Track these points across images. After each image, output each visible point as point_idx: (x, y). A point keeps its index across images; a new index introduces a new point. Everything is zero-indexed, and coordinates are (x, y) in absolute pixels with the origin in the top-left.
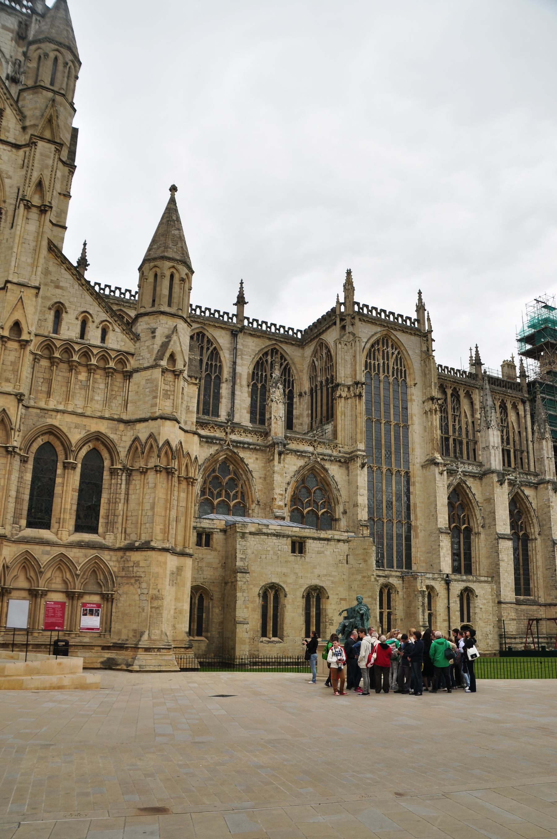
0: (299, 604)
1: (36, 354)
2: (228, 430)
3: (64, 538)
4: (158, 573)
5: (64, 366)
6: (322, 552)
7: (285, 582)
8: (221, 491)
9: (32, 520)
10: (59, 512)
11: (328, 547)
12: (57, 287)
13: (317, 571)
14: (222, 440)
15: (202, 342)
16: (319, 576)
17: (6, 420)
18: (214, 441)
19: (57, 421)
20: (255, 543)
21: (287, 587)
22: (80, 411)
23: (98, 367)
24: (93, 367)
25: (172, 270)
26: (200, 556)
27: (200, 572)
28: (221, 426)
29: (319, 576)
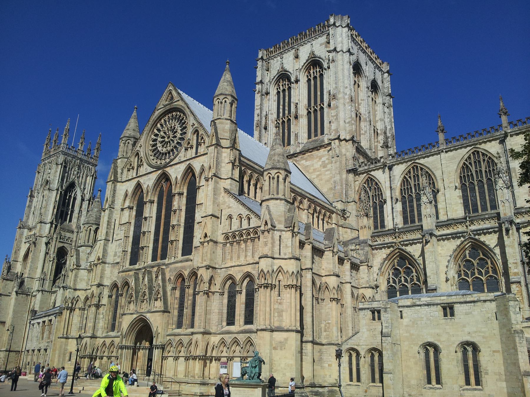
0: (453, 357)
1: (223, 243)
2: (468, 223)
4: (260, 343)
6: (471, 313)
7: (439, 341)
8: (474, 270)
11: (475, 308)
12: (229, 208)
13: (467, 330)
14: (464, 233)
15: (479, 157)
16: (470, 333)
18: (458, 235)
19: (232, 272)
20: (412, 313)
21: (441, 344)
25: (269, 175)
26: (374, 327)
27: (375, 339)
28: (462, 222)
29: (470, 333)
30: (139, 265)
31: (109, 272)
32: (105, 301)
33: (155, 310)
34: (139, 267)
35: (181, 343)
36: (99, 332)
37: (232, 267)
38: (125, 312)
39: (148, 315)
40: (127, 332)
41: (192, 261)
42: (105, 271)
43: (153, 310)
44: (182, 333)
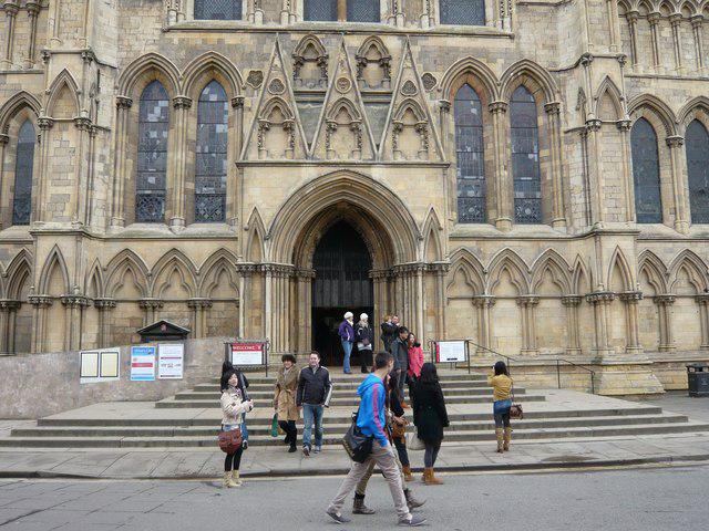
3: (686, 230)
5: (643, 23)
9: (640, 212)
10: (672, 198)
17: (612, 89)
19: (652, 88)
22: (674, 74)
23: (683, 19)
24: (678, 18)
30: (264, 21)
31: (113, 23)
32: (106, 116)
33: (400, 160)
34: (265, 27)
35: (508, 262)
36: (94, 217)
37: (650, 77)
38: (253, 157)
39: (377, 173)
40: (280, 221)
41: (511, 37)
42: (101, 15)
43: (392, 161)
44: (510, 234)
